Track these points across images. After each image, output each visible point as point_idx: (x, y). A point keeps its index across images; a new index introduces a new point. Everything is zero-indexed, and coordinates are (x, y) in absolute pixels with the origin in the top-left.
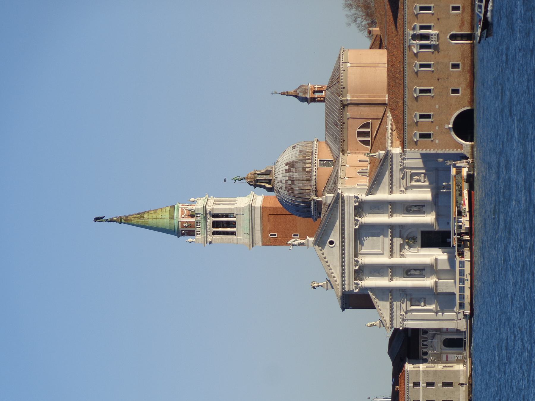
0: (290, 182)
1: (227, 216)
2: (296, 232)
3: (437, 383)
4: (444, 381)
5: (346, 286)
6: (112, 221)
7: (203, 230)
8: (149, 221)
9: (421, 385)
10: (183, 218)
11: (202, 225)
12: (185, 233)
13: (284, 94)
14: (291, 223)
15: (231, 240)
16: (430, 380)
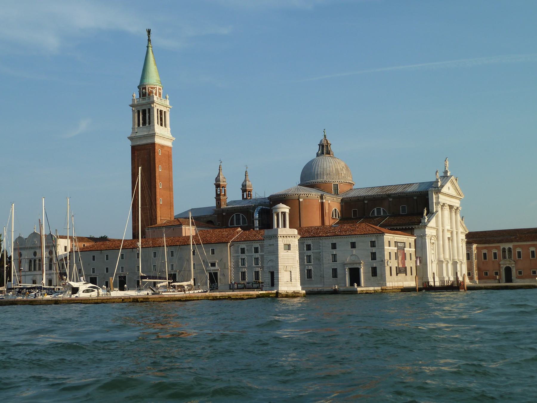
6: (149, 40)
9: (410, 249)
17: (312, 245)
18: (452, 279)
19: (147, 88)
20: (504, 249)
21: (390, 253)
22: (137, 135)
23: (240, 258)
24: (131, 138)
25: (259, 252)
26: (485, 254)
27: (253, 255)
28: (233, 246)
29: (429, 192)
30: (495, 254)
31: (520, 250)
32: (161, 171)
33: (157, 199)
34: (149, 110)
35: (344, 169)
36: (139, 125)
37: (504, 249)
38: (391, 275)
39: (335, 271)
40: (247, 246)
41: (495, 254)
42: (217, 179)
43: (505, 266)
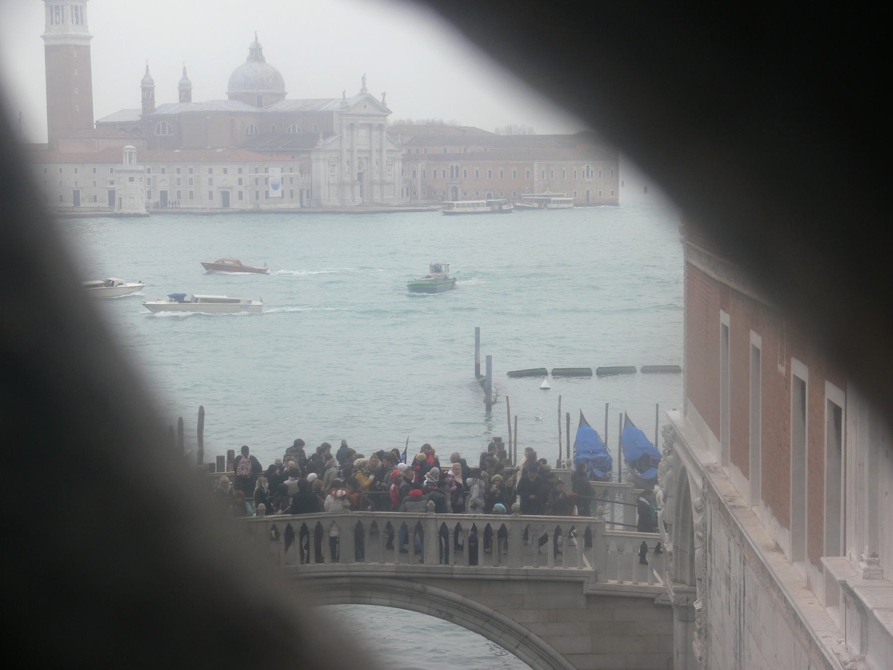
13: (185, 69)
17: (193, 169)
18: (358, 200)
20: (452, 167)
21: (257, 179)
22: (51, 34)
24: (44, 37)
26: (435, 172)
29: (334, 113)
32: (76, 75)
34: (62, 6)
36: (52, 23)
37: (452, 167)
38: (257, 198)
39: (211, 193)
41: (444, 171)
42: (143, 82)
43: (452, 186)
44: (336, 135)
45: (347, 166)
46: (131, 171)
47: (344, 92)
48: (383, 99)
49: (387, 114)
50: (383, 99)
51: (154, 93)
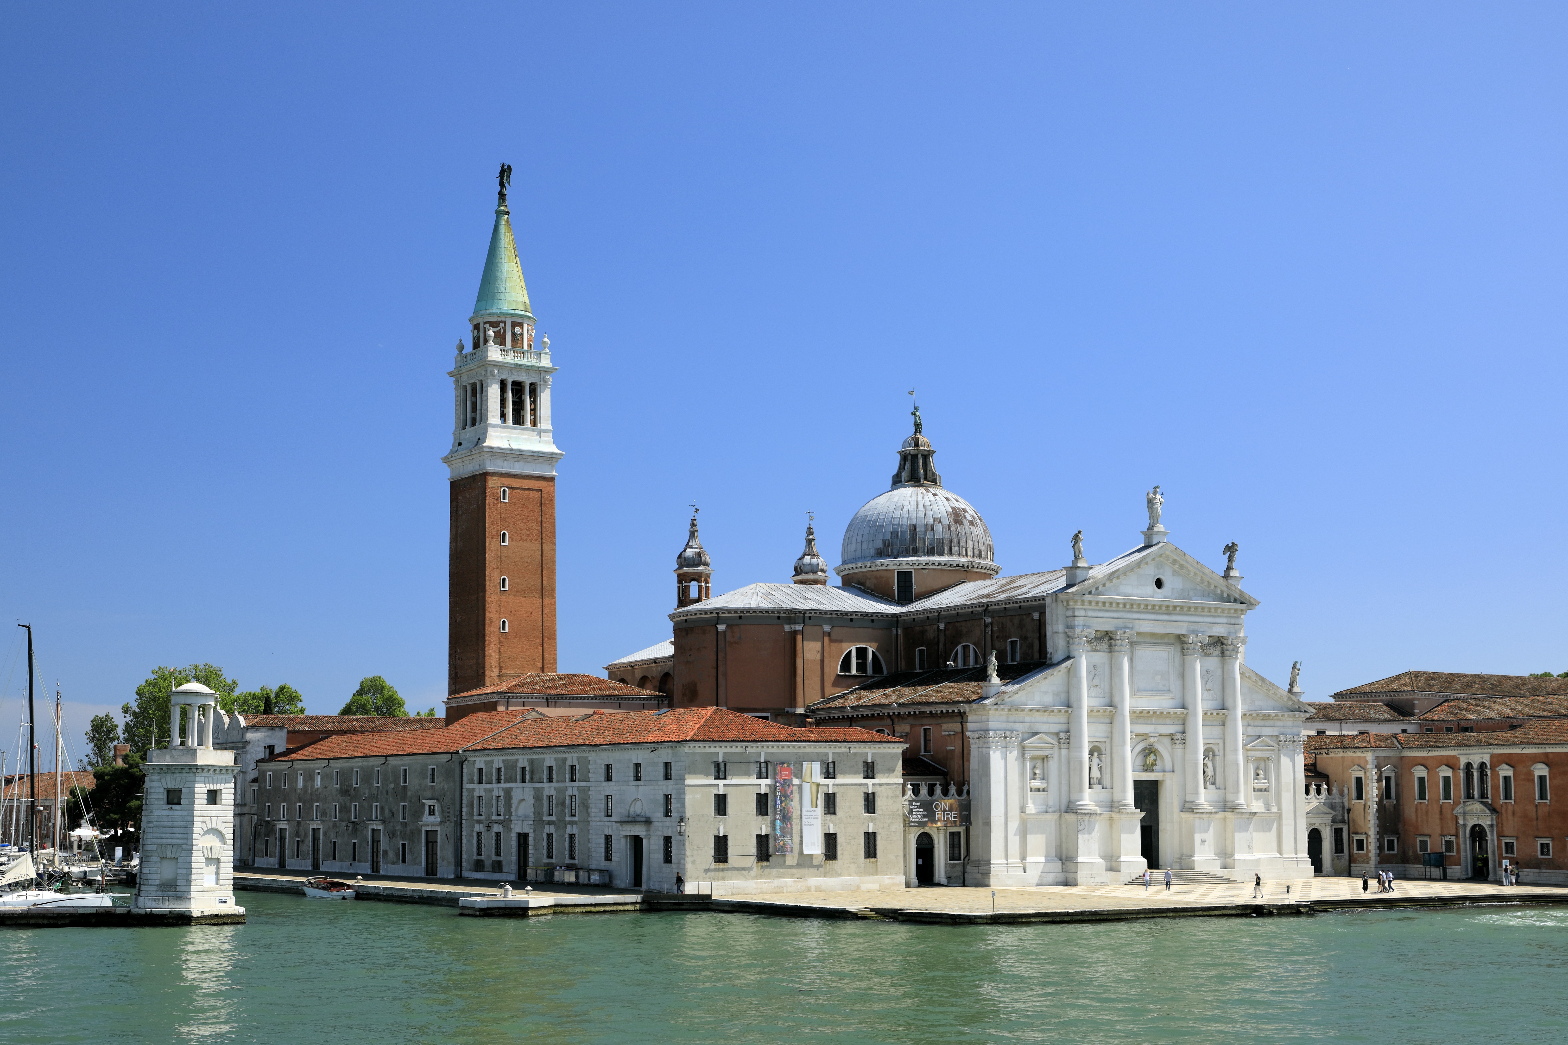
0: (969, 518)
1: (534, 410)
2: (511, 539)
3: (875, 819)
4: (878, 838)
5: (1082, 613)
6: (502, 195)
7: (512, 361)
8: (515, 265)
10: (528, 331)
11: (520, 361)
12: (498, 329)
13: (810, 532)
14: (527, 530)
15: (493, 414)
16: (879, 804)
17: (577, 767)
19: (481, 326)
20: (1469, 766)
23: (476, 794)
25: (502, 781)
26: (1421, 780)
27: (491, 790)
28: (466, 762)
29: (1048, 601)
30: (1447, 780)
31: (1509, 772)
32: (507, 544)
33: (487, 621)
35: (938, 527)
37: (1469, 766)
40: (486, 762)
43: (1470, 824)
44: (1052, 665)
45: (1095, 760)
46: (170, 768)
47: (1076, 538)
48: (1229, 568)
49: (1239, 606)
50: (1229, 568)
51: (707, 588)
